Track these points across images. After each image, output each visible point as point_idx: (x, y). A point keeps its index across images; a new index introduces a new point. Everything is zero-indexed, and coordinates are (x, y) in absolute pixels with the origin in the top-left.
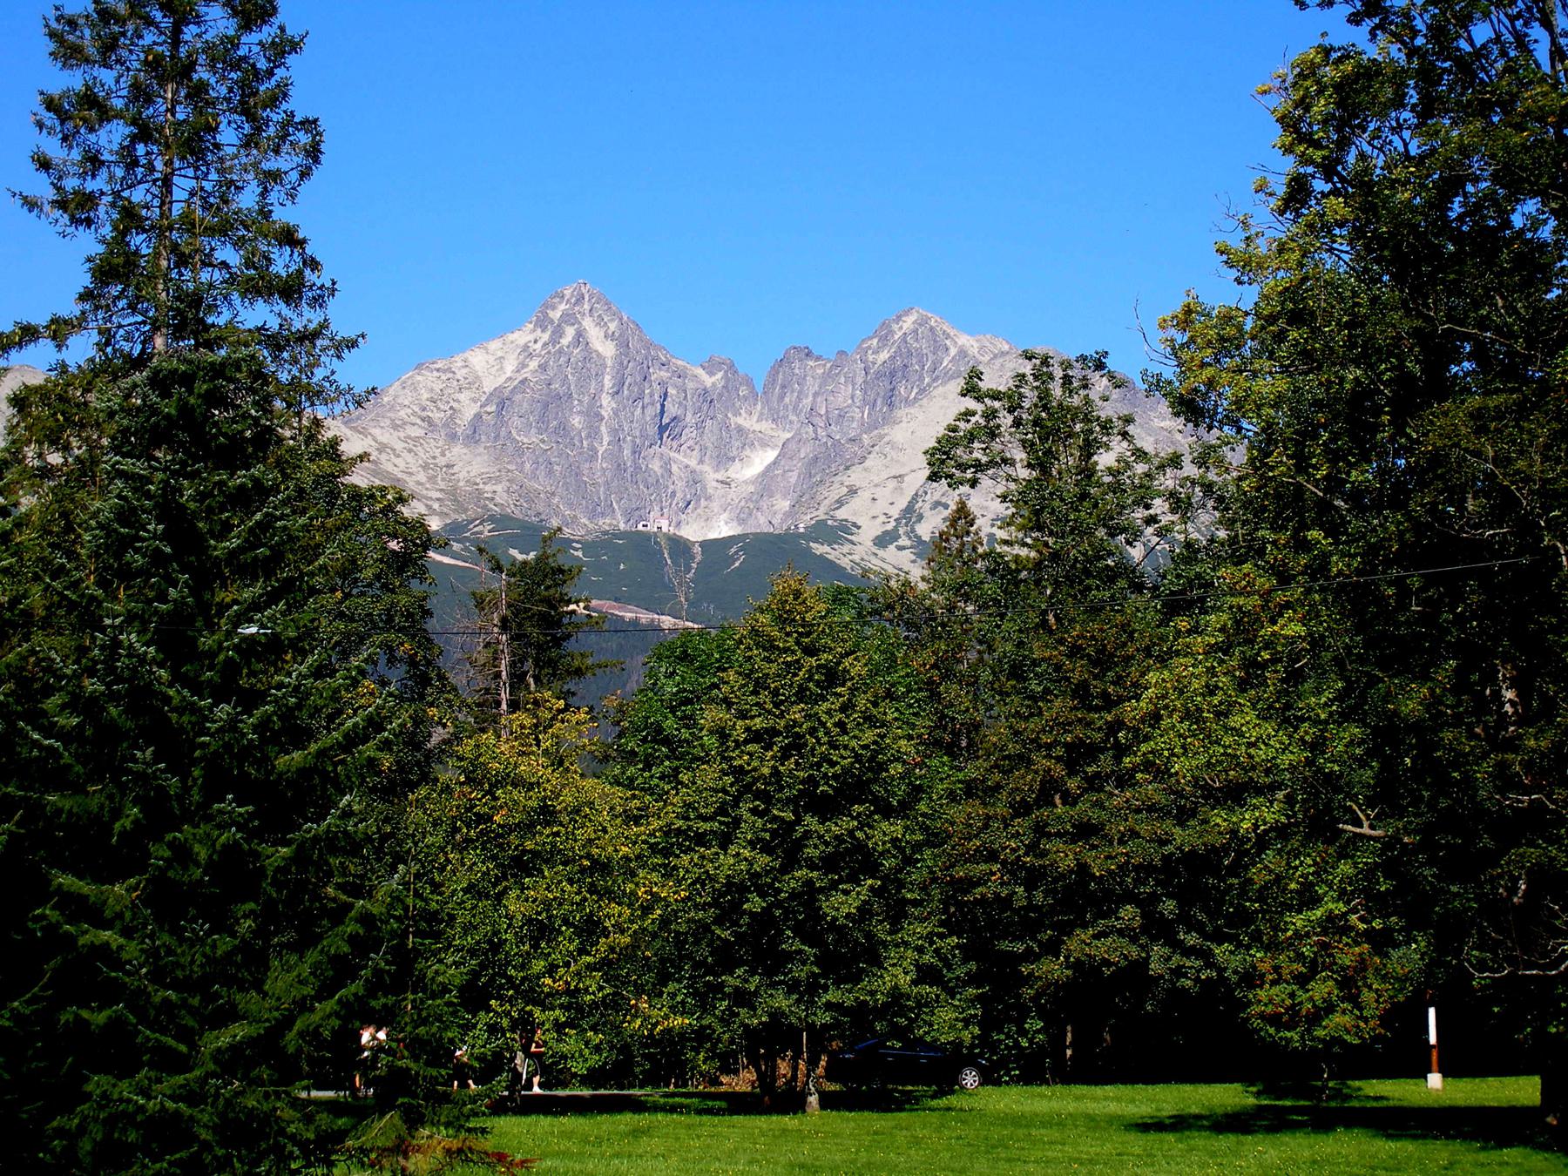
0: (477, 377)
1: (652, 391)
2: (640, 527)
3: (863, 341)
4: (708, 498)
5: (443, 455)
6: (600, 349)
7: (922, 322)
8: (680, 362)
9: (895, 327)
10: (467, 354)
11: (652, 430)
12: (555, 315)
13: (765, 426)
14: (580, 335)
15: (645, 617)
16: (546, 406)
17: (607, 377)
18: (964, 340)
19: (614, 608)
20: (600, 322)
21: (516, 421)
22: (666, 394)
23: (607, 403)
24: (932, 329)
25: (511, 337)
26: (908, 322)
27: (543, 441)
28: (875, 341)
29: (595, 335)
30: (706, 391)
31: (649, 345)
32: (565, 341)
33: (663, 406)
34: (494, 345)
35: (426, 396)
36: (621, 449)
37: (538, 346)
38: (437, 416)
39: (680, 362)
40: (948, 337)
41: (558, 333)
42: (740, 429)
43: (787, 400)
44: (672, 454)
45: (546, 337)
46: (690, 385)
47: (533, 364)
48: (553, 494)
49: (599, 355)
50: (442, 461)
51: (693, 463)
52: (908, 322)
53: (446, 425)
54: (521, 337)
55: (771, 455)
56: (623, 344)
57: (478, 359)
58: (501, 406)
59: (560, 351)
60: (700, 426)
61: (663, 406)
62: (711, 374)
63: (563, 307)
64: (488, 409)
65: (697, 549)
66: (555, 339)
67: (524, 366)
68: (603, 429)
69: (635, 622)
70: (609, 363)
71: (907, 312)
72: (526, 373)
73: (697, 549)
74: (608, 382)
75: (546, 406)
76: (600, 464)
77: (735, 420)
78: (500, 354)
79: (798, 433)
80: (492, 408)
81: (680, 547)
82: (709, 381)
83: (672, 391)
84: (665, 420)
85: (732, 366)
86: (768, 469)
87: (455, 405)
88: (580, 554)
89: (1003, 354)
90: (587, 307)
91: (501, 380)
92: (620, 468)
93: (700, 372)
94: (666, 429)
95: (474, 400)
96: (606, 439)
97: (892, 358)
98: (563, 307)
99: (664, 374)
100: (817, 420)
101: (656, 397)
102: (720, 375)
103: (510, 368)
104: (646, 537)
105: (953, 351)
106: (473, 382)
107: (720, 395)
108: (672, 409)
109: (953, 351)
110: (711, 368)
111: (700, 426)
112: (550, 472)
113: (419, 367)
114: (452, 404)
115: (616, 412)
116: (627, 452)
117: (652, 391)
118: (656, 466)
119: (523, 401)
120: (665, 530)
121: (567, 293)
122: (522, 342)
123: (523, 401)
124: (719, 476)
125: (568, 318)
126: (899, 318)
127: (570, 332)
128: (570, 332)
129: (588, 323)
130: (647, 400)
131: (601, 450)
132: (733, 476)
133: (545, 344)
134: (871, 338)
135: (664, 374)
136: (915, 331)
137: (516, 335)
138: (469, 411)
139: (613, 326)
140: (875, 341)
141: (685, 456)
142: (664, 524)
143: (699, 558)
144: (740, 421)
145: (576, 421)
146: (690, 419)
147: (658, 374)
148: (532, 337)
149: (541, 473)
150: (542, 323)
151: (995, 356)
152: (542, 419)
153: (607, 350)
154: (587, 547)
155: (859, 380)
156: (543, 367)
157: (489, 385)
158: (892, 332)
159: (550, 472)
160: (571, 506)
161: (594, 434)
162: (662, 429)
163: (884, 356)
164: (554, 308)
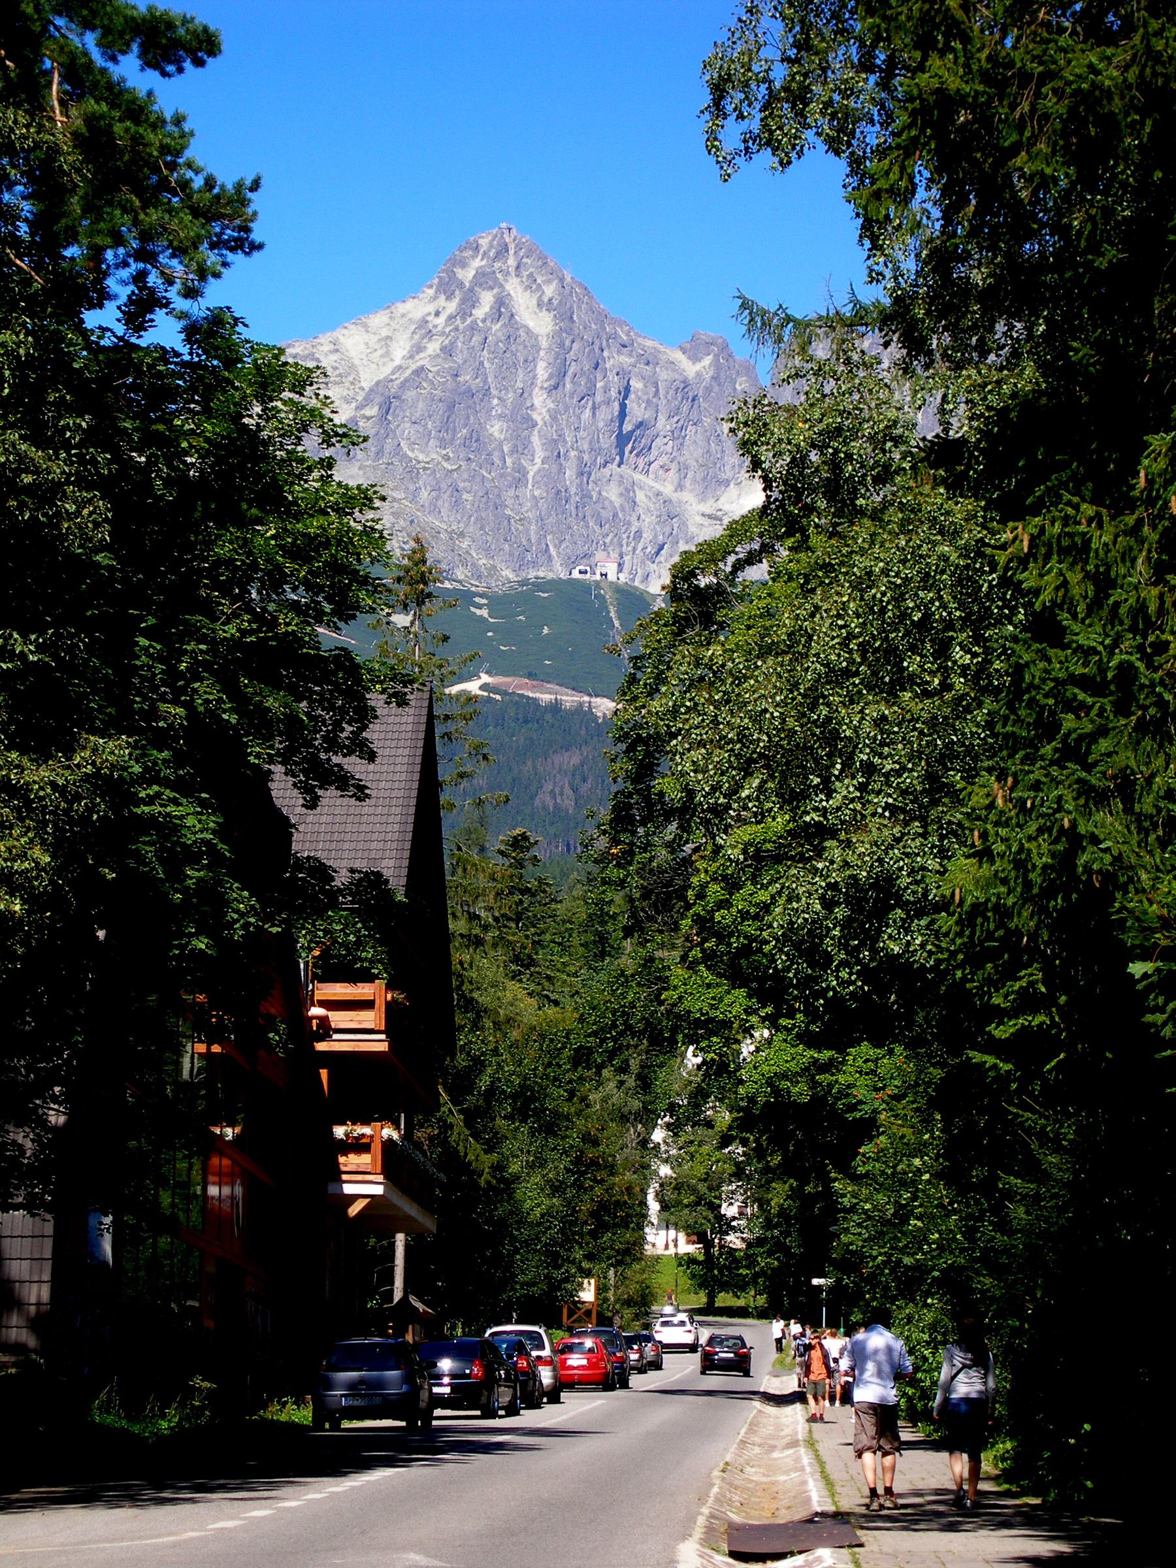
0: (352, 367)
1: (607, 385)
2: (576, 574)
8: (649, 343)
10: (338, 334)
11: (608, 442)
12: (467, 275)
14: (502, 305)
15: (569, 699)
16: (451, 407)
19: (525, 686)
20: (532, 285)
22: (627, 389)
23: (541, 403)
25: (401, 308)
27: (448, 459)
29: (523, 303)
30: (686, 384)
31: (602, 318)
32: (480, 313)
33: (623, 406)
34: (378, 320)
36: (561, 470)
37: (441, 320)
39: (649, 343)
41: (470, 300)
44: (637, 477)
45: (452, 307)
46: (664, 375)
47: (433, 347)
48: (462, 535)
49: (528, 331)
51: (668, 489)
54: (416, 308)
56: (563, 313)
58: (386, 408)
59: (473, 328)
60: (678, 435)
61: (623, 406)
62: (695, 359)
63: (477, 263)
64: (368, 412)
67: (418, 349)
68: (536, 440)
69: (555, 708)
70: (544, 343)
72: (422, 360)
74: (542, 371)
75: (451, 407)
76: (533, 490)
78: (385, 332)
82: (691, 369)
83: (636, 384)
84: (627, 427)
85: (725, 347)
88: (484, 613)
90: (512, 262)
91: (386, 371)
92: (559, 496)
93: (679, 356)
94: (628, 440)
98: (477, 263)
99: (625, 360)
101: (614, 393)
102: (707, 361)
103: (399, 351)
104: (583, 588)
107: (708, 390)
108: (637, 411)
110: (694, 351)
111: (678, 435)
112: (457, 504)
115: (554, 416)
116: (570, 473)
117: (607, 385)
118: (613, 494)
119: (417, 402)
120: (612, 577)
121: (484, 242)
122: (417, 315)
123: (417, 402)
124: (707, 508)
125: (484, 279)
127: (487, 299)
128: (487, 299)
129: (513, 286)
130: (599, 398)
131: (532, 471)
132: (726, 507)
133: (451, 318)
135: (625, 360)
137: (410, 305)
139: (550, 290)
141: (656, 478)
142: (611, 569)
145: (496, 429)
147: (615, 360)
148: (431, 308)
149: (445, 504)
150: (447, 287)
152: (446, 425)
153: (541, 324)
154: (497, 602)
156: (448, 351)
159: (457, 504)
160: (487, 551)
161: (521, 447)
162: (622, 440)
164: (464, 265)
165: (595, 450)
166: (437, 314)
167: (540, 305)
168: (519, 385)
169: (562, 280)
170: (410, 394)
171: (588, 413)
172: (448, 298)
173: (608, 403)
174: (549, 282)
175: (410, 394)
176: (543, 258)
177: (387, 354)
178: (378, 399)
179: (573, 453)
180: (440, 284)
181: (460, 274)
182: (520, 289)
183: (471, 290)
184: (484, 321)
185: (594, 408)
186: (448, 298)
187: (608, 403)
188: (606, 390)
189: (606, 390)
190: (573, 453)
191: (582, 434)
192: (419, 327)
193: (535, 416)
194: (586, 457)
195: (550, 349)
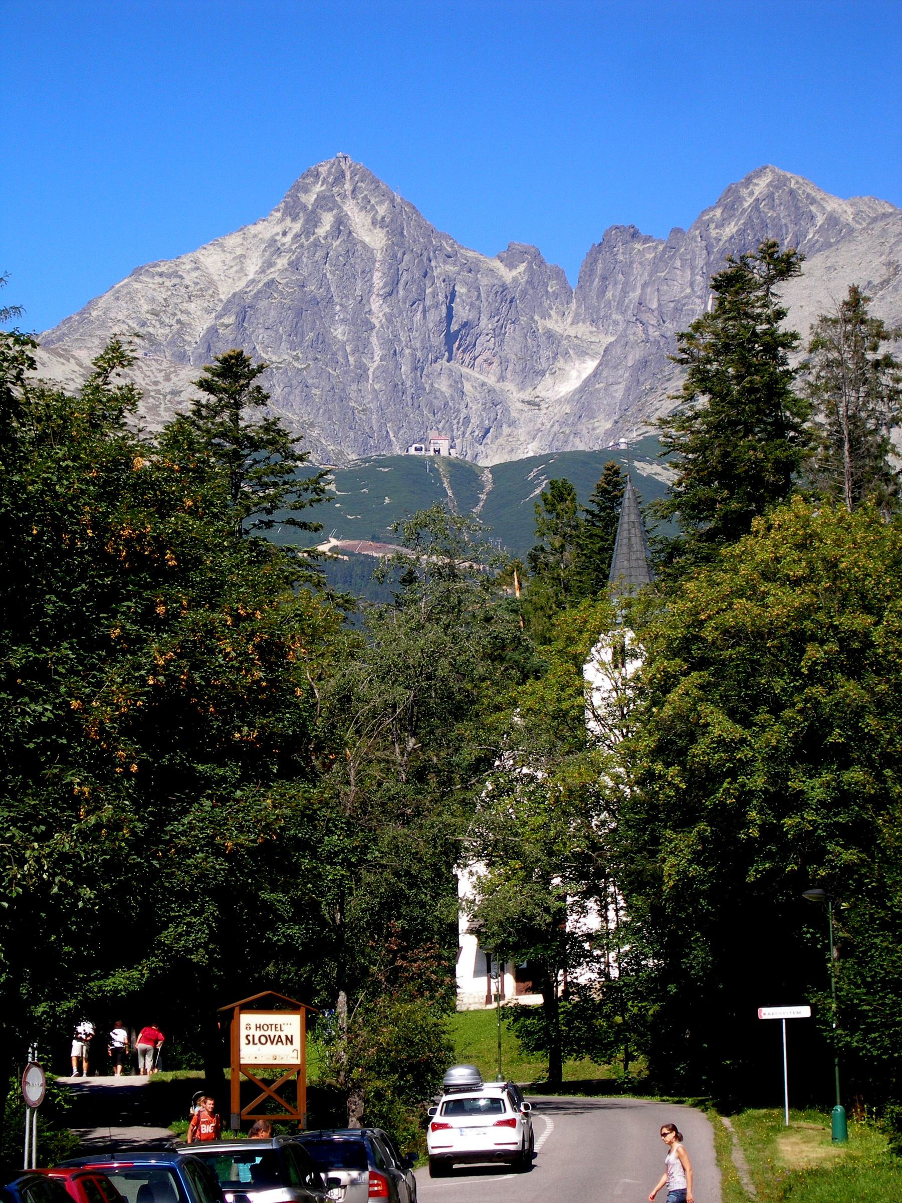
0: (211, 282)
1: (436, 291)
2: (412, 451)
3: (704, 213)
4: (512, 423)
5: (167, 379)
6: (367, 240)
7: (780, 183)
8: (470, 254)
9: (744, 192)
10: (200, 254)
11: (438, 340)
12: (309, 199)
13: (583, 330)
14: (341, 226)
16: (299, 313)
17: (377, 275)
18: (833, 204)
20: (366, 206)
21: (262, 334)
22: (453, 294)
23: (377, 307)
24: (791, 192)
25: (253, 230)
26: (761, 185)
27: (296, 358)
28: (718, 212)
30: (504, 287)
31: (429, 232)
32: (321, 231)
33: (450, 309)
34: (233, 241)
35: (146, 307)
36: (398, 366)
37: (288, 239)
38: (161, 332)
39: (470, 254)
40: (813, 201)
41: (313, 221)
42: (550, 335)
43: (609, 295)
44: (465, 370)
45: (297, 227)
46: (484, 281)
47: (282, 262)
48: (312, 425)
49: (365, 246)
50: (166, 387)
51: (491, 380)
52: (761, 185)
53: (172, 343)
54: (266, 229)
55: (591, 365)
56: (394, 229)
57: (212, 260)
58: (242, 317)
59: (316, 244)
60: (498, 333)
61: (450, 309)
62: (511, 266)
63: (318, 188)
65: (487, 477)
66: (308, 231)
67: (270, 264)
68: (374, 340)
70: (379, 256)
71: (759, 173)
72: (273, 274)
73: (487, 477)
74: (378, 280)
75: (299, 313)
76: (372, 384)
77: (543, 324)
78: (239, 251)
79: (624, 335)
80: (230, 320)
81: (464, 474)
82: (508, 275)
83: (461, 290)
84: (454, 327)
85: (537, 255)
86: (587, 382)
87: (184, 318)
89: (885, 216)
90: (348, 186)
91: (241, 284)
92: (397, 388)
94: (455, 339)
95: (208, 311)
96: (378, 353)
97: (742, 232)
98: (318, 188)
99: (450, 268)
100: (645, 317)
101: (441, 298)
102: (522, 267)
103: (252, 267)
104: (418, 462)
105: (820, 220)
106: (207, 287)
107: (524, 293)
108: (462, 313)
109: (820, 220)
110: (510, 259)
111: (498, 333)
112: (308, 398)
113: (137, 272)
114: (180, 316)
115: (389, 318)
117: (436, 291)
118: (443, 386)
119: (269, 310)
120: (444, 453)
121: (324, 170)
122: (267, 236)
123: (269, 310)
124: (526, 395)
125: (325, 203)
126: (748, 181)
127: (328, 219)
128: (328, 219)
129: (350, 208)
130: (428, 302)
131: (372, 368)
132: (543, 394)
133: (297, 236)
134: (712, 209)
135: (450, 268)
136: (771, 196)
137: (260, 227)
138: (201, 326)
140: (718, 212)
141: (481, 371)
142: (444, 446)
143: (489, 487)
144: (550, 324)
145: (339, 332)
146: (486, 325)
147: (441, 268)
148: (279, 229)
149: (296, 400)
150: (293, 210)
151: (875, 220)
152: (296, 330)
153: (375, 240)
154: (343, 478)
155: (700, 262)
156: (295, 265)
157: (225, 292)
158: (740, 199)
159: (308, 398)
160: (335, 438)
162: (450, 338)
163: (731, 229)
164: (306, 191)
165: (427, 348)
166: (285, 234)
167: (374, 223)
168: (359, 293)
169: (392, 201)
170: (263, 304)
171: (419, 315)
172: (294, 220)
173: (437, 306)
174: (381, 202)
175: (263, 304)
176: (375, 182)
177: (242, 270)
178: (235, 309)
179: (407, 351)
180: (286, 207)
181: (303, 198)
182: (356, 210)
183: (313, 211)
184: (325, 238)
185: (424, 311)
186: (294, 220)
187: (437, 306)
188: (434, 295)
189: (434, 295)
190: (407, 351)
191: (415, 334)
192: (269, 246)
193: (375, 321)
194: (419, 354)
195: (383, 262)
